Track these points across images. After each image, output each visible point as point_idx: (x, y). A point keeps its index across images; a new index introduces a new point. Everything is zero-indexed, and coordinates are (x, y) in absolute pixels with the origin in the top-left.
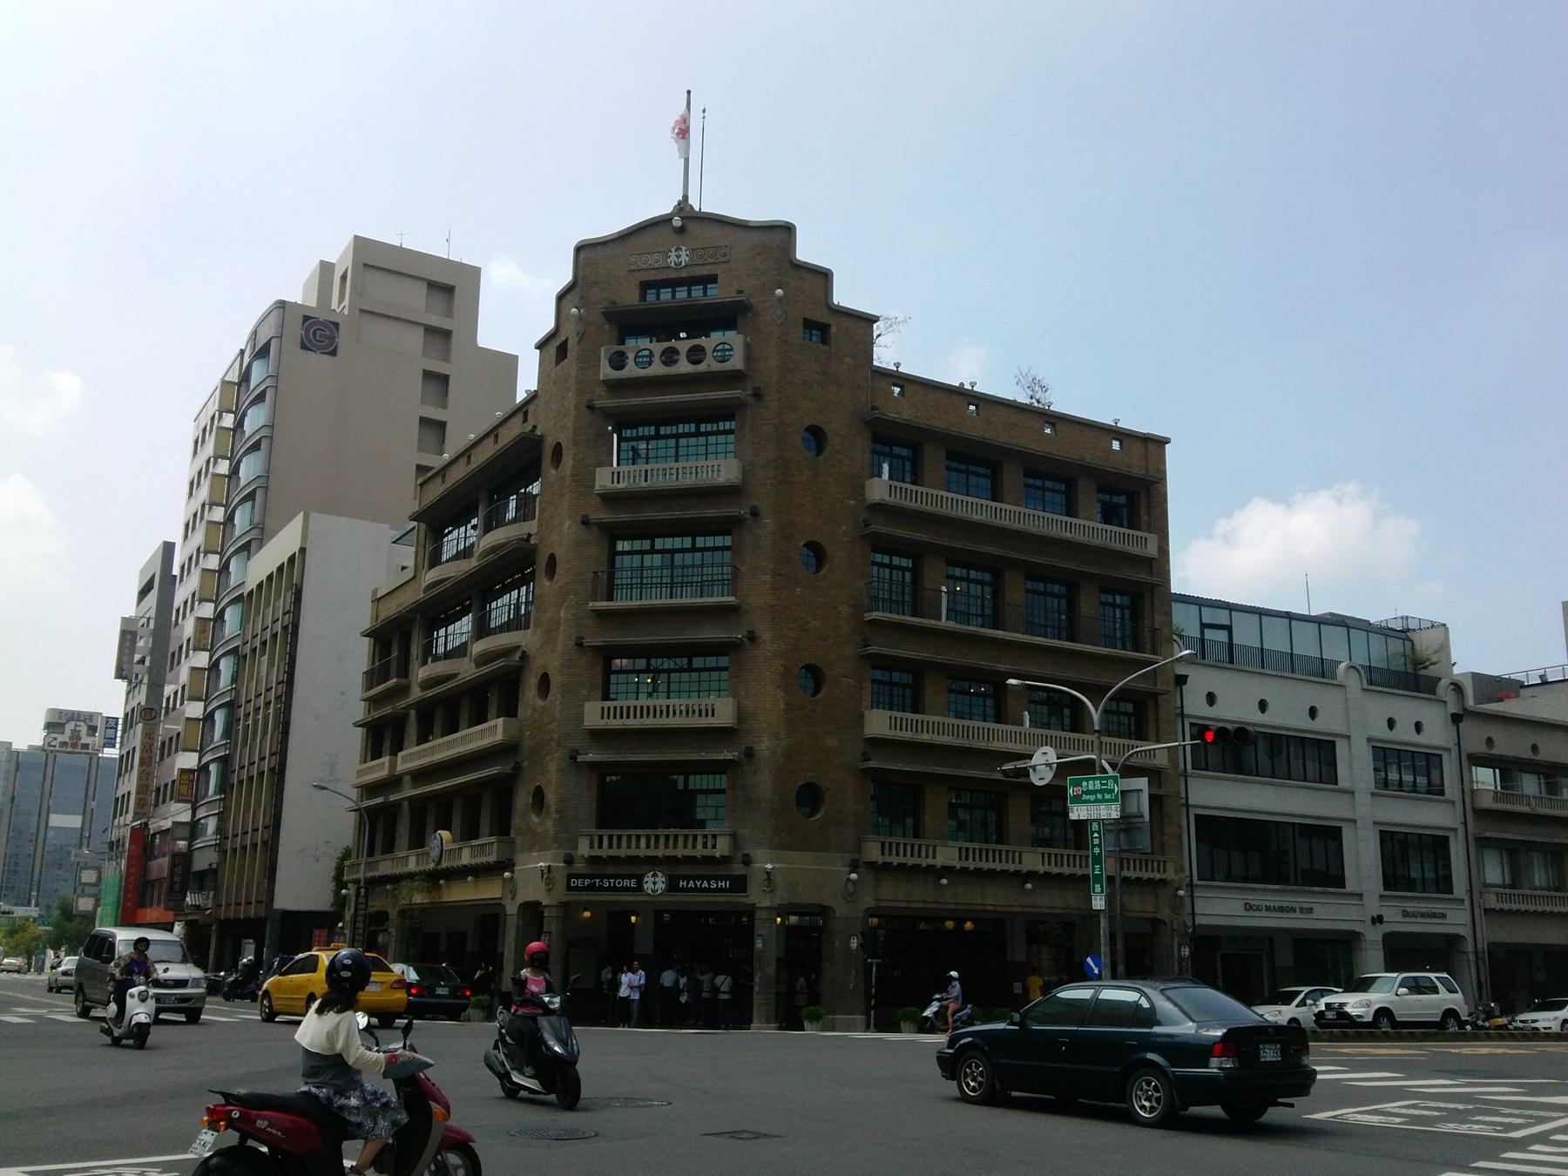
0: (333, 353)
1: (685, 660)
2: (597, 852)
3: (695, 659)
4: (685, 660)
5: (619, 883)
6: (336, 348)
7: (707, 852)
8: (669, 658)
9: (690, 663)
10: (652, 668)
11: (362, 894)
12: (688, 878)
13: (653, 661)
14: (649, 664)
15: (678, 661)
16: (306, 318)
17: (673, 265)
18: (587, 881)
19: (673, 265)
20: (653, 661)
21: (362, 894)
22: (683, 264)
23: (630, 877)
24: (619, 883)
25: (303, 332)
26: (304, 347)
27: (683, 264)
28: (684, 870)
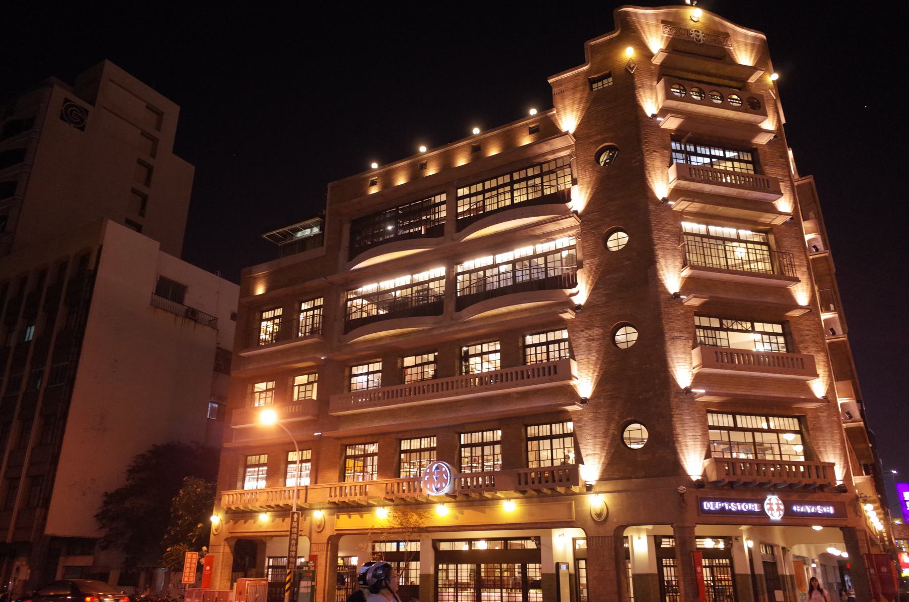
0: (82, 129)
1: (749, 325)
2: (734, 479)
3: (756, 324)
4: (749, 325)
5: (745, 507)
6: (85, 126)
7: (819, 482)
8: (737, 321)
9: (753, 326)
10: (724, 327)
11: (295, 520)
12: (801, 503)
13: (724, 321)
14: (721, 324)
15: (744, 324)
16: (66, 100)
17: (695, 40)
18: (719, 505)
19: (695, 40)
20: (724, 321)
21: (295, 520)
22: (702, 42)
23: (752, 501)
24: (745, 507)
25: (63, 108)
26: (62, 118)
27: (702, 42)
28: (794, 497)
